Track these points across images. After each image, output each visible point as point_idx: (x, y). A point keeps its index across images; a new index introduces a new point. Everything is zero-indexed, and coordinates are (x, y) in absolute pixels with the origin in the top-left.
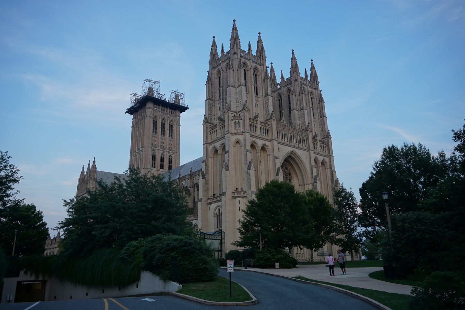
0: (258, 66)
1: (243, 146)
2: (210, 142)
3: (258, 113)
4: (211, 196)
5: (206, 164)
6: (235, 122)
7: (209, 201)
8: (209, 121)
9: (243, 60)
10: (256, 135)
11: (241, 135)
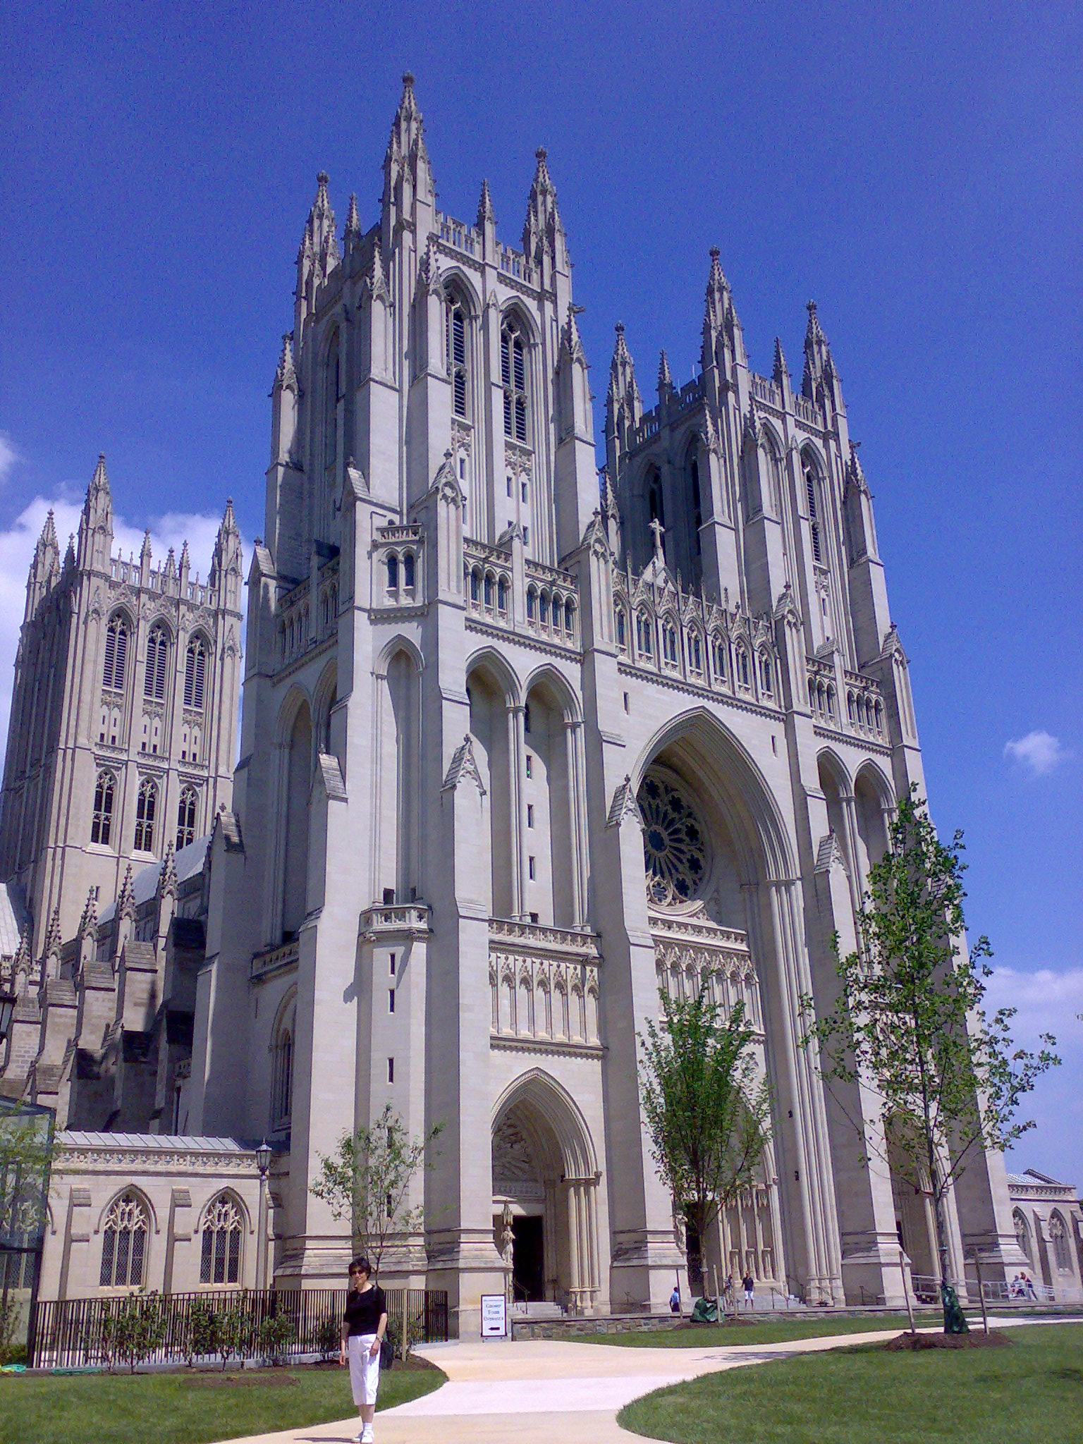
0: (532, 304)
2: (278, 667)
4: (268, 941)
5: (249, 774)
7: (258, 967)
9: (444, 264)
10: (502, 624)
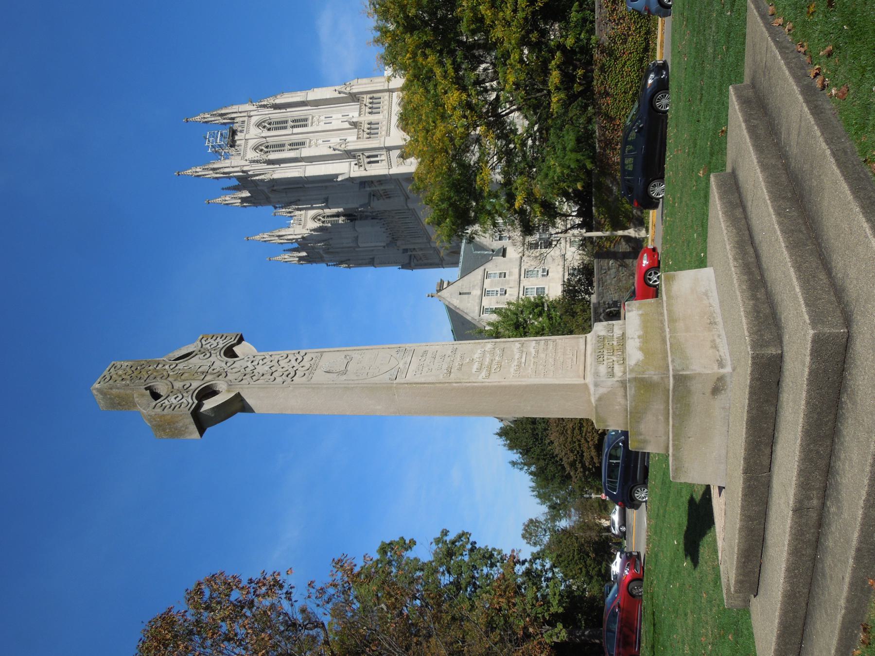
0: (254, 120)
3: (341, 117)
8: (367, 201)
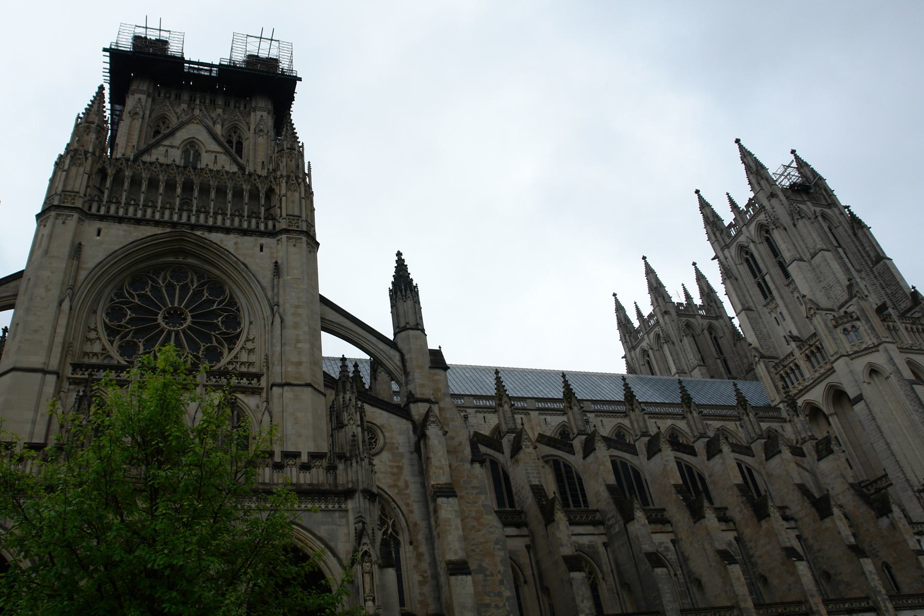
1: (891, 376)
6: (845, 330)
11: (874, 354)
